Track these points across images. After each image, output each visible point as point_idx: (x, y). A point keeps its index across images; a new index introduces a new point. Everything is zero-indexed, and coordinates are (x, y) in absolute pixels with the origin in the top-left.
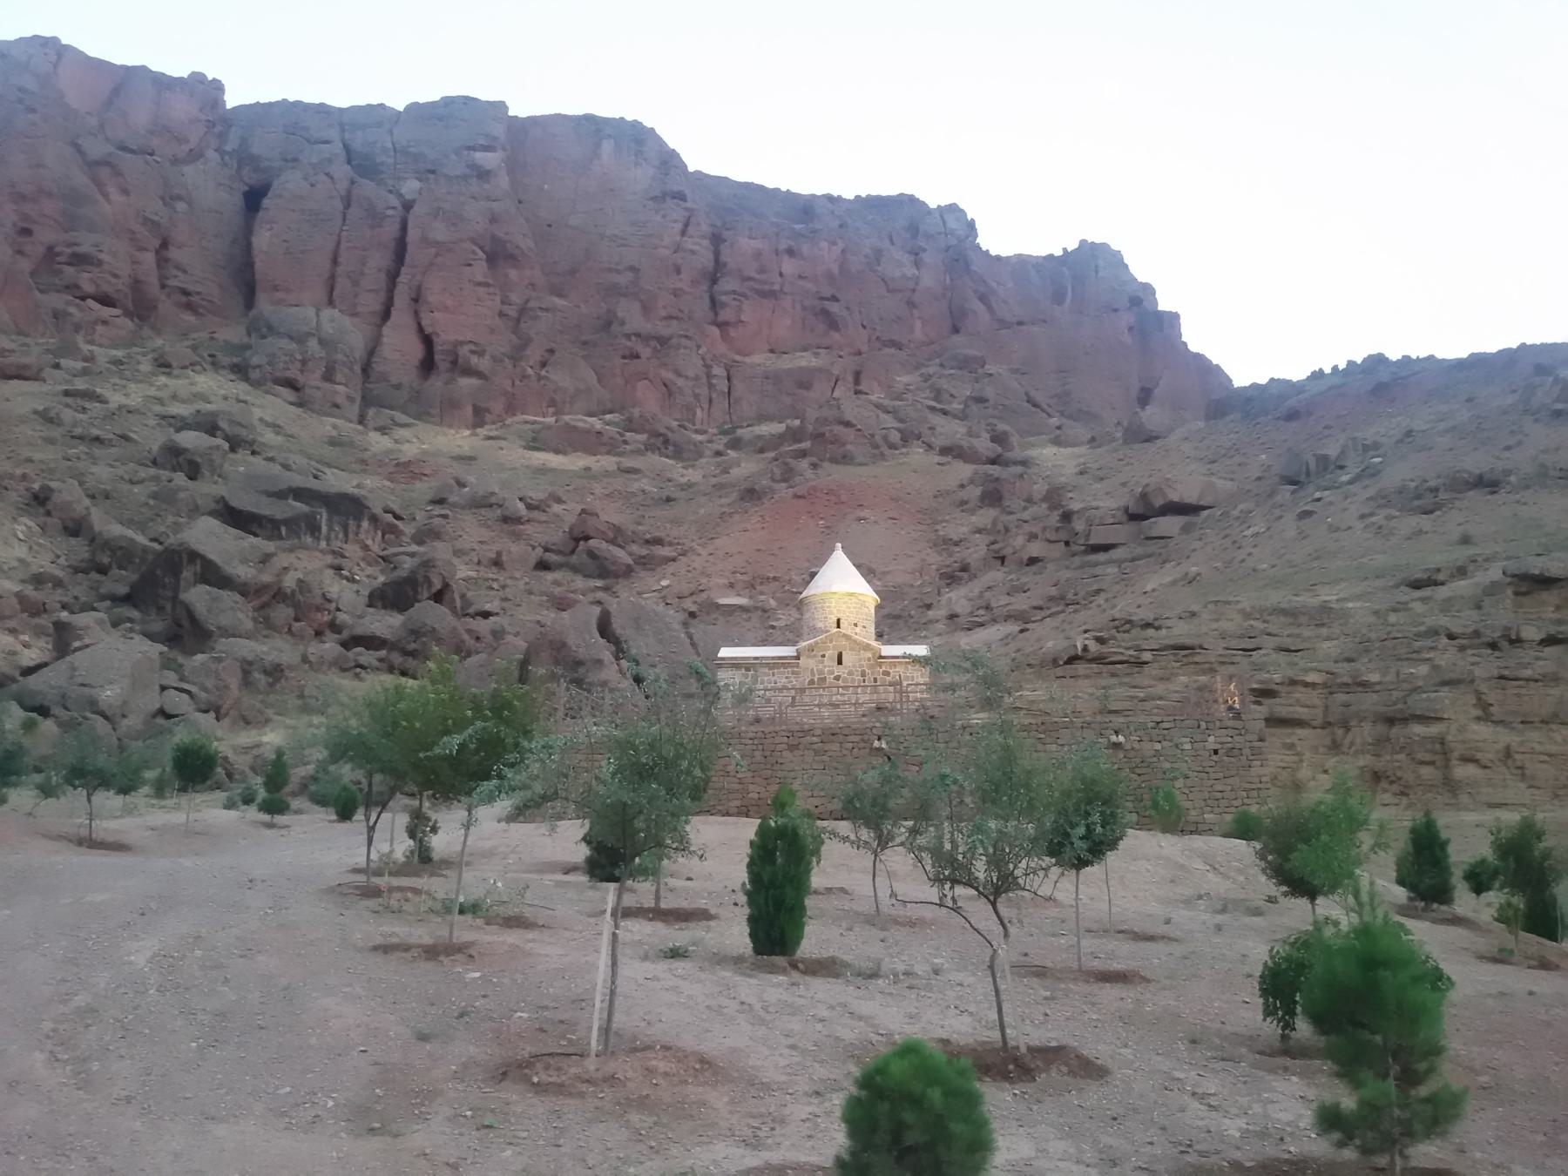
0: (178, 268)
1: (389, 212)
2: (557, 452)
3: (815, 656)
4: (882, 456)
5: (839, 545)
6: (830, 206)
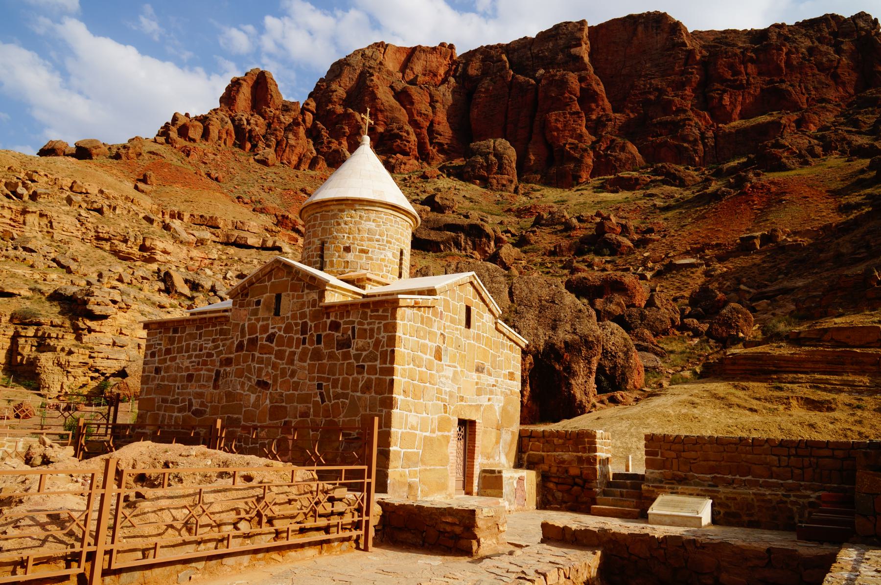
0: (437, 134)
1: (530, 87)
2: (612, 192)
3: (249, 305)
4: (806, 163)
5: (367, 139)
6: (777, 30)
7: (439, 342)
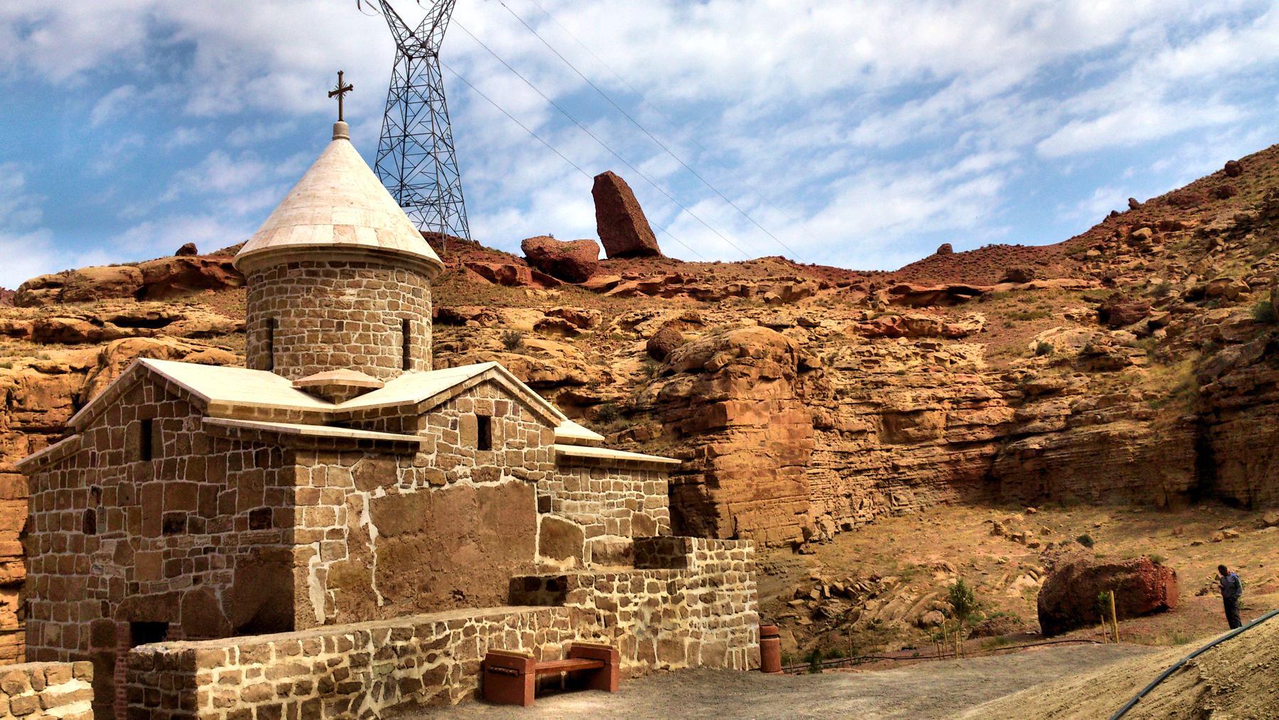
7: (90, 505)
